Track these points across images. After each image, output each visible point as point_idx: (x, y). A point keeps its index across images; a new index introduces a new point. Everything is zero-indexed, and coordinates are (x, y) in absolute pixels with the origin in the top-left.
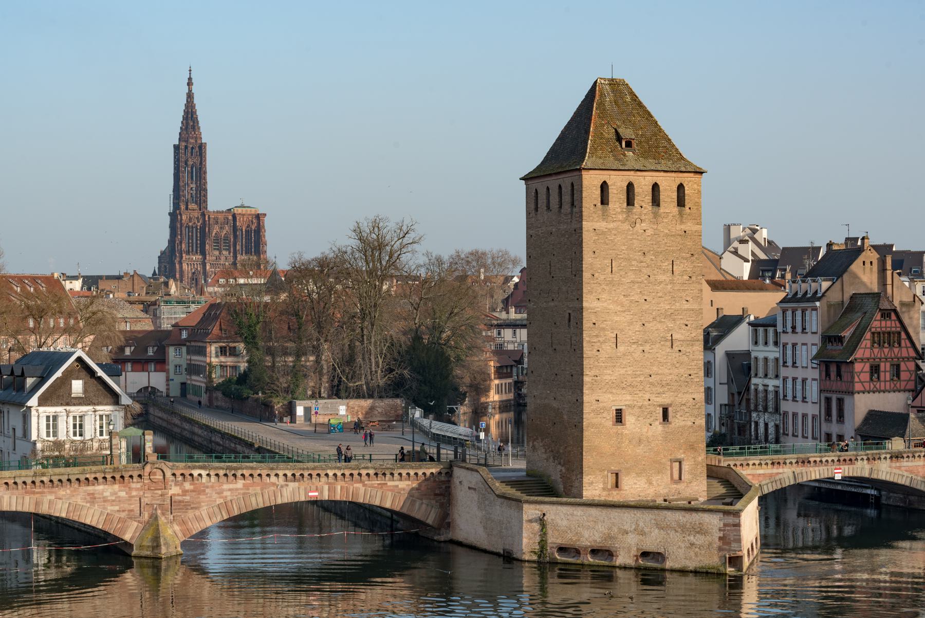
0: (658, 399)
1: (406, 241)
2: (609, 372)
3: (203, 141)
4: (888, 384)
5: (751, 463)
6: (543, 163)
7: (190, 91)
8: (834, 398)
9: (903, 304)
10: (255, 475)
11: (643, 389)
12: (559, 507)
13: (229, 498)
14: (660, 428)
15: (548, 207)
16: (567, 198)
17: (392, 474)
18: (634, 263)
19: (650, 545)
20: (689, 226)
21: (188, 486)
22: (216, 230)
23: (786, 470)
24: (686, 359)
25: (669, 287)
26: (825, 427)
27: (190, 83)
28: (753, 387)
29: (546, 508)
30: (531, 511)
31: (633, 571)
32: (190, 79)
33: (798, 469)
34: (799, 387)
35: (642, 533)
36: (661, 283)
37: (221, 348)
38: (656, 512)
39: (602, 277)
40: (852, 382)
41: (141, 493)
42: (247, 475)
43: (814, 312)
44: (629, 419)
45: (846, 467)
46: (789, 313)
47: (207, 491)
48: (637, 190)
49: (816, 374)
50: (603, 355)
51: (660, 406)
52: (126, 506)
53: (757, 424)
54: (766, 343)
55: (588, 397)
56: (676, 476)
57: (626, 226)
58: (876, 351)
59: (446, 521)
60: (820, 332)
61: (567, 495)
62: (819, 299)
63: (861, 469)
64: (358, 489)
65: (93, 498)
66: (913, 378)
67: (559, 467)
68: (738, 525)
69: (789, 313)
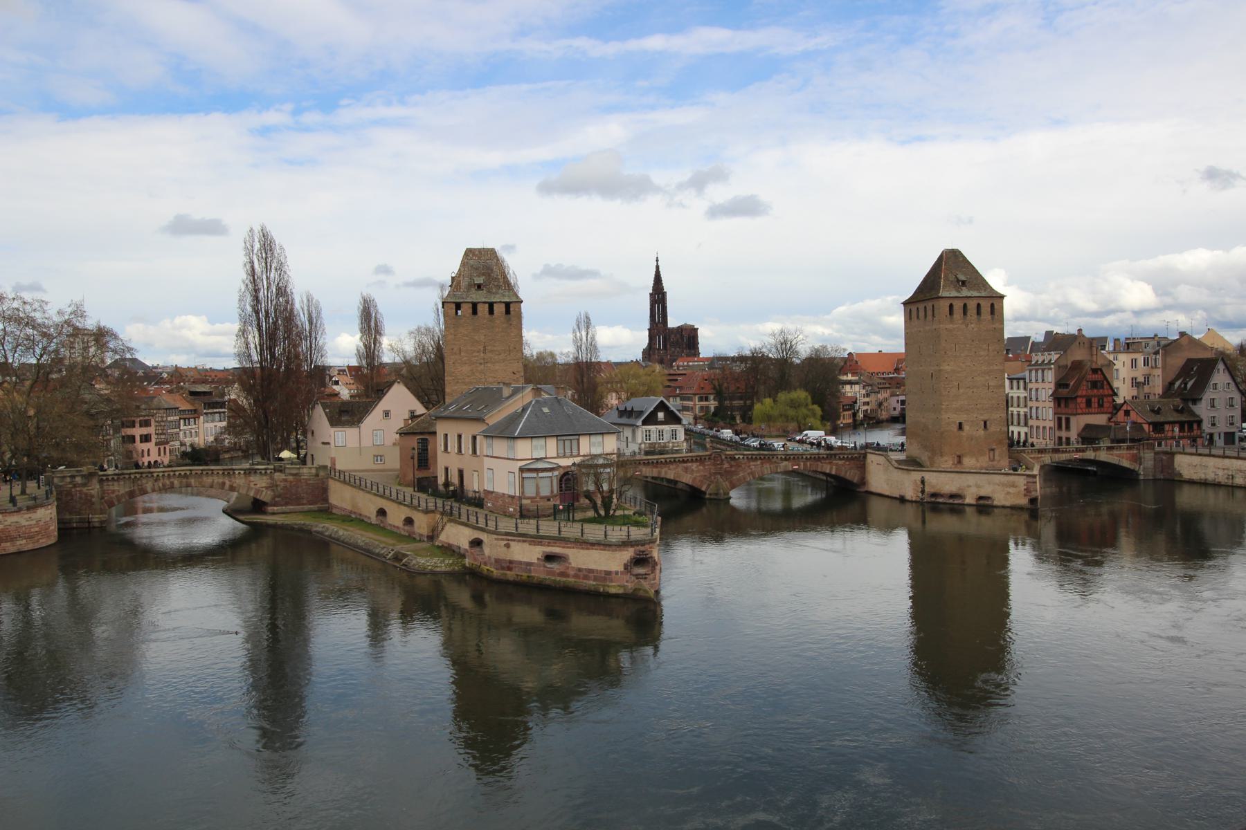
1: (799, 339)
2: (954, 403)
3: (665, 290)
4: (1096, 410)
6: (914, 294)
7: (657, 264)
8: (1063, 418)
9: (1102, 366)
10: (767, 457)
12: (931, 473)
13: (753, 470)
14: (983, 432)
15: (918, 317)
16: (929, 313)
17: (835, 457)
18: (968, 346)
19: (983, 493)
20: (997, 325)
21: (733, 463)
22: (673, 336)
23: (1047, 455)
25: (987, 358)
26: (1058, 434)
27: (657, 261)
28: (1010, 412)
29: (923, 474)
30: (916, 476)
31: (975, 507)
32: (657, 258)
34: (1040, 411)
35: (978, 486)
36: (982, 356)
37: (701, 397)
38: (986, 475)
39: (951, 353)
40: (1076, 408)
41: (710, 467)
42: (762, 457)
43: (1050, 371)
44: (966, 427)
45: (1081, 454)
46: (1033, 372)
47: (743, 466)
48: (969, 307)
49: (1052, 404)
52: (702, 473)
53: (1013, 432)
54: (1018, 388)
55: (945, 416)
56: (992, 456)
57: (964, 326)
58: (1089, 391)
59: (863, 481)
60: (1054, 382)
61: (932, 467)
62: (1053, 364)
63: (1090, 455)
64: (818, 465)
65: (686, 469)
66: (1111, 406)
67: (927, 453)
68: (1036, 482)
69: (1033, 372)
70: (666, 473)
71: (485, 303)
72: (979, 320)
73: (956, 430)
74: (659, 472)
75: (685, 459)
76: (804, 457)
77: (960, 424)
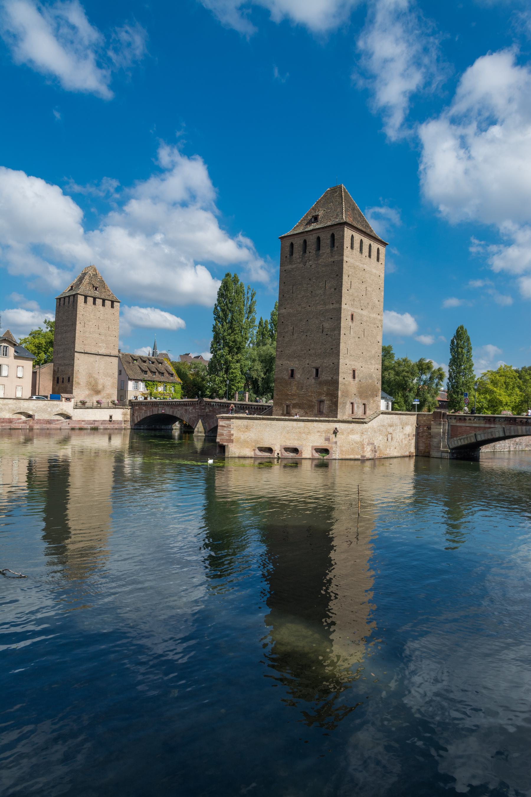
0: (313, 364)
5: (467, 418)
11: (305, 358)
14: (313, 381)
21: (211, 409)
23: (496, 426)
24: (330, 339)
33: (508, 427)
39: (288, 296)
44: (298, 376)
47: (216, 411)
50: (287, 339)
51: (314, 368)
52: (195, 415)
57: (301, 265)
70: (176, 413)
71: (67, 296)
72: (318, 256)
73: (287, 378)
74: (173, 412)
75: (185, 403)
76: (253, 407)
77: (292, 371)
